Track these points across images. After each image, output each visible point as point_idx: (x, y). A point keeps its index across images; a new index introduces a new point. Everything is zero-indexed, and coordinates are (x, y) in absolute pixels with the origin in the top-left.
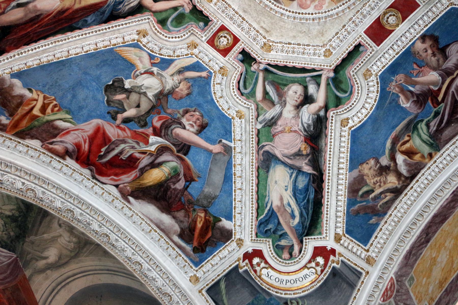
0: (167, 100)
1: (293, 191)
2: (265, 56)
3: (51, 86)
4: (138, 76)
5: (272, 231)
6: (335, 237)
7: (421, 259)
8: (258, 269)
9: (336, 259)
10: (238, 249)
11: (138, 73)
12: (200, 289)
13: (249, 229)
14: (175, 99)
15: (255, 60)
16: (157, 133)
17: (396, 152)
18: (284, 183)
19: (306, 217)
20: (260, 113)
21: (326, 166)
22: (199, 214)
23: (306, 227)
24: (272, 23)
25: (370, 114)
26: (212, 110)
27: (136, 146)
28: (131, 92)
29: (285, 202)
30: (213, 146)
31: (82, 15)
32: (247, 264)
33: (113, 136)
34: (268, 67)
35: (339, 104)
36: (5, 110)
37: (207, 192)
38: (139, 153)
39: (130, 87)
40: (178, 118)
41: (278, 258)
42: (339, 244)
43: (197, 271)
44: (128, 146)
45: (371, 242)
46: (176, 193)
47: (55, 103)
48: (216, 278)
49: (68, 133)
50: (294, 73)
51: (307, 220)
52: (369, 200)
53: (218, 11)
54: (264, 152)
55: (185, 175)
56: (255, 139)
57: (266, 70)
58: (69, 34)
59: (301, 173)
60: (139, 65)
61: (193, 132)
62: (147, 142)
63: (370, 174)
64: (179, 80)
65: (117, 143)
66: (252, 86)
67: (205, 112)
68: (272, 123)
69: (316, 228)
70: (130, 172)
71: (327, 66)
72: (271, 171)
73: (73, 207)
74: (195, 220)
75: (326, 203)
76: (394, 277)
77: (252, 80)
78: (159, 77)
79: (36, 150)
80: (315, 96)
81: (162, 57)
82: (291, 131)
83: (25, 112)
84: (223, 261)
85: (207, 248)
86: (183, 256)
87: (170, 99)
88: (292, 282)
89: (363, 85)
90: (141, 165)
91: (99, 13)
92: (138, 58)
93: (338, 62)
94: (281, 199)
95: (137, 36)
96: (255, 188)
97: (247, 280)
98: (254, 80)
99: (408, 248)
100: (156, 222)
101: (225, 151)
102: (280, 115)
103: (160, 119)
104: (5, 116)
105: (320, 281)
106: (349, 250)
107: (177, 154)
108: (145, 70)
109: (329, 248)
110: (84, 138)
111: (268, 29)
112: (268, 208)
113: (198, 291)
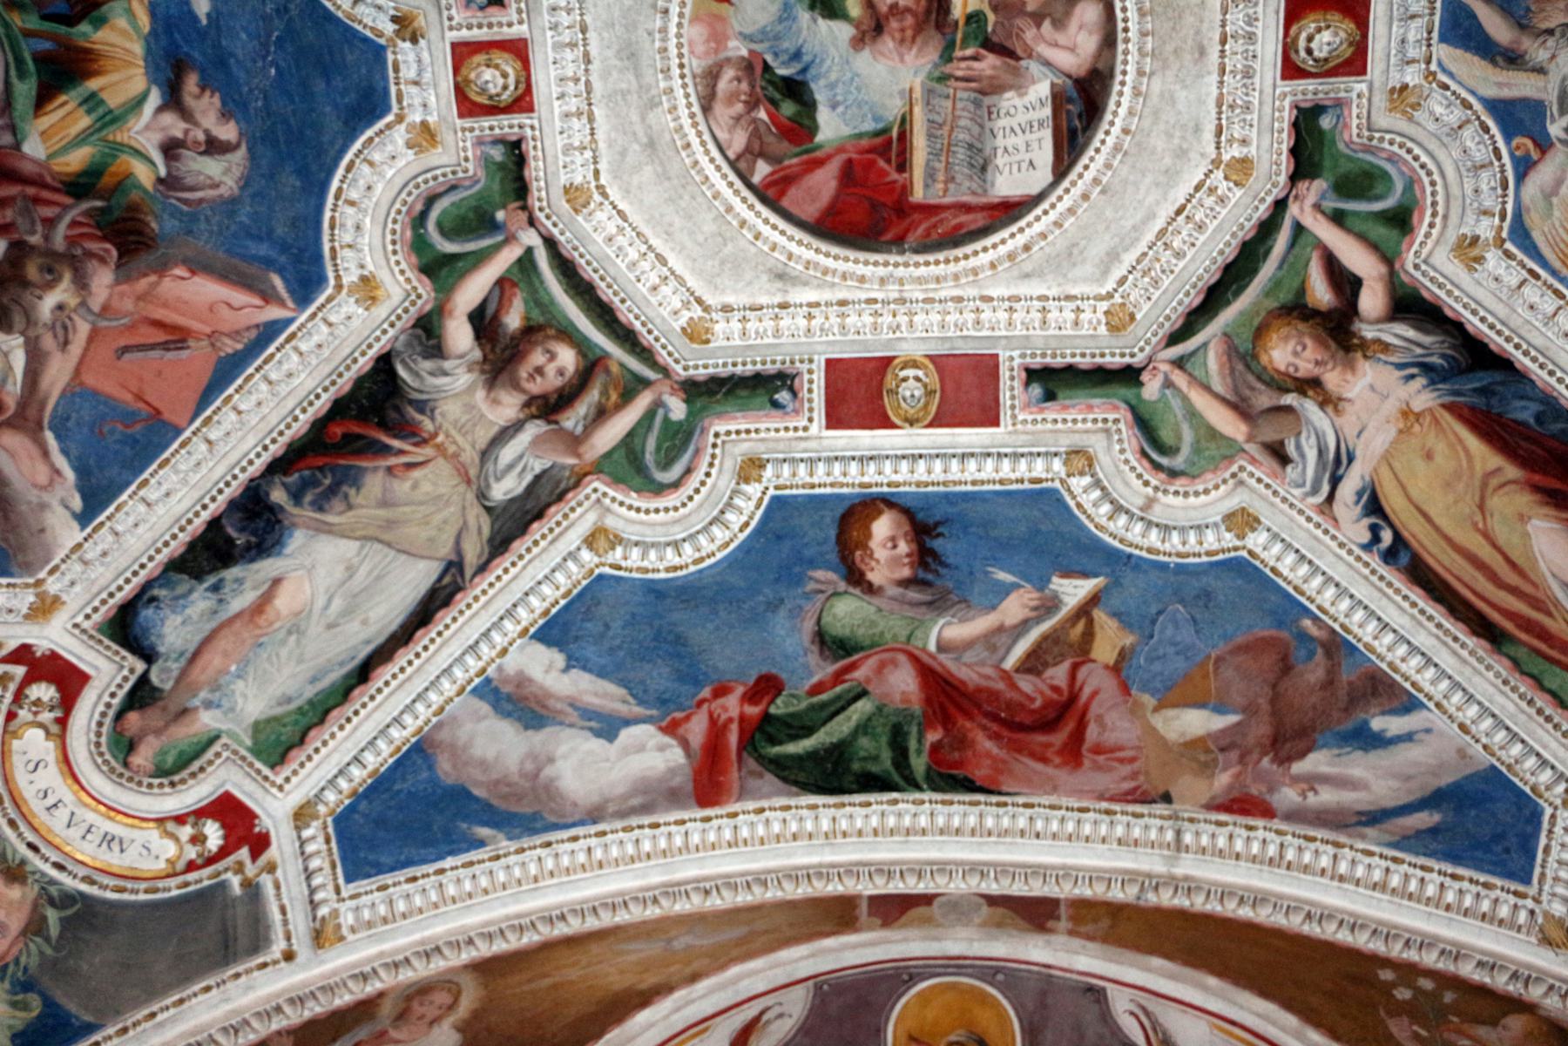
31: (1527, 438)
53: (1255, 123)
81: (1501, 144)
91: (1494, 401)
92: (1555, 200)
95: (1488, 255)
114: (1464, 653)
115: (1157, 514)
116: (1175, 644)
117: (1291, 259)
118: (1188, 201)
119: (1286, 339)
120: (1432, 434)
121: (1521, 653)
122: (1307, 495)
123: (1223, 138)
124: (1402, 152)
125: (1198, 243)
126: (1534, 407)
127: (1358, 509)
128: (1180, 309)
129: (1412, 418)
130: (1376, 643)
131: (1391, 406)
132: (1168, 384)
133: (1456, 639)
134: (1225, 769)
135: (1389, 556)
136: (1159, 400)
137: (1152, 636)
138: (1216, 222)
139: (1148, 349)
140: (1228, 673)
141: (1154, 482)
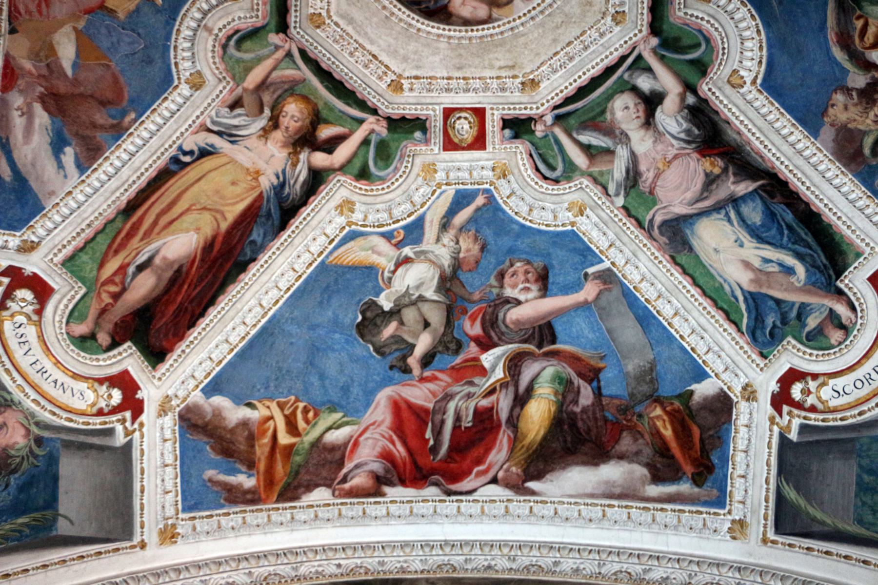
0: (461, 282)
1: (752, 237)
2: (537, 98)
3: (277, 379)
4: (390, 279)
5: (778, 323)
8: (811, 400)
11: (386, 274)
12: (761, 536)
13: (742, 357)
14: (470, 270)
15: (530, 119)
16: (486, 345)
17: (863, 54)
18: (729, 239)
19: (810, 251)
20: (604, 182)
21: (769, 160)
22: (652, 415)
23: (825, 266)
24: (509, 51)
25: (764, 41)
26: (535, 241)
27: (472, 389)
28: (399, 311)
29: (757, 263)
30: (582, 292)
31: (242, 235)
32: (789, 413)
33: (425, 401)
34: (556, 112)
35: (703, 69)
36: (235, 462)
37: (634, 369)
38: (484, 397)
39: (392, 305)
40: (498, 295)
43: (730, 512)
44: (460, 400)
46: (590, 414)
47: (301, 405)
48: (767, 490)
49: (356, 444)
50: (600, 85)
51: (815, 255)
54: (659, 227)
55: (580, 375)
56: (631, 225)
57: (558, 119)
58: (246, 277)
59: (740, 201)
60: (379, 261)
61: (536, 298)
62: (483, 372)
63: (853, 115)
64: (454, 239)
65: (440, 408)
66: (560, 159)
67: (526, 253)
68: (633, 177)
69: (842, 253)
70: (495, 439)
71: (635, 35)
72: (695, 243)
73: (446, 558)
74: (654, 431)
75: (821, 206)
77: (553, 150)
78: (422, 257)
79: (329, 505)
80: (657, 87)
82: (670, 162)
83: (267, 449)
85: (712, 457)
86: (687, 508)
87: (463, 276)
89: (712, 12)
90: (504, 415)
91: (263, 219)
92: (370, 252)
93: (646, 17)
94: (747, 265)
95: (343, 218)
96: (694, 291)
98: (556, 148)
100: (600, 492)
101: (605, 283)
102: (634, 158)
103: (473, 319)
104: (242, 473)
107: (542, 351)
108: (393, 262)
110: (387, 436)
111: (510, 63)
112: (741, 298)
114: (118, 194)
115: (202, 34)
116: (118, 42)
117: (345, 117)
118: (380, 62)
119: (301, 112)
120: (245, 185)
121: (118, 224)
122: (212, 119)
123: (413, 80)
124: (400, 173)
125: (357, 65)
126: (259, 240)
127: (203, 145)
128: (320, 55)
129: (255, 176)
130: (122, 150)
131: (261, 165)
132: (277, 48)
133: (126, 190)
134: (34, 66)
135: (175, 160)
136: (268, 42)
137: (123, 29)
138: (368, 74)
139: (299, 37)
140: (100, 71)
141: (221, 35)
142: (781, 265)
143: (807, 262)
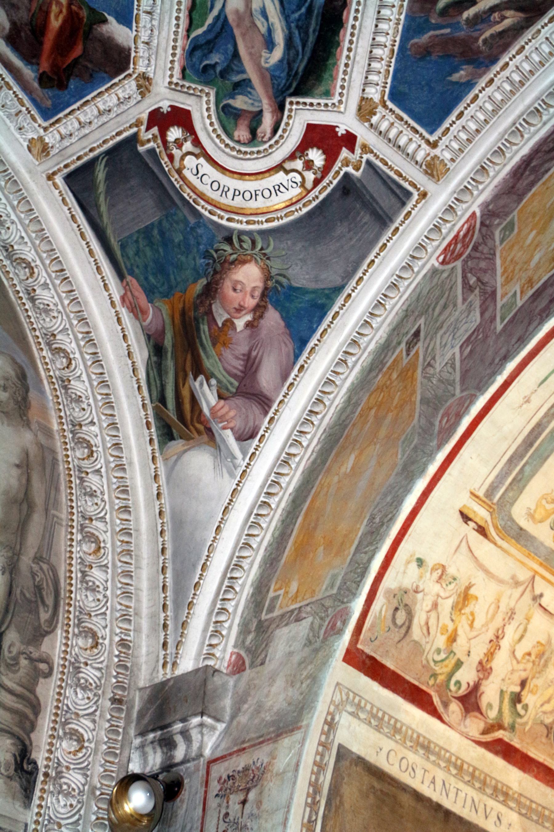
5: (218, 69)
6: (360, 109)
7: (544, 184)
8: (177, 153)
9: (354, 157)
10: (139, 98)
19: (300, 49)
23: (297, 73)
32: (155, 137)
41: (224, 137)
42: (366, 124)
45: (446, 124)
48: (86, 154)
51: (300, 57)
52: (459, 23)
69: (319, 79)
75: (351, 22)
76: (478, 214)
84: (104, 119)
85: (72, 81)
86: (16, 88)
88: (247, 195)
97: (153, 172)
99: (525, 150)
105: (310, 201)
106: (390, 140)
109: (341, 131)
112: (215, 12)
113: (44, 176)
142: (270, 31)
143: (288, 54)
